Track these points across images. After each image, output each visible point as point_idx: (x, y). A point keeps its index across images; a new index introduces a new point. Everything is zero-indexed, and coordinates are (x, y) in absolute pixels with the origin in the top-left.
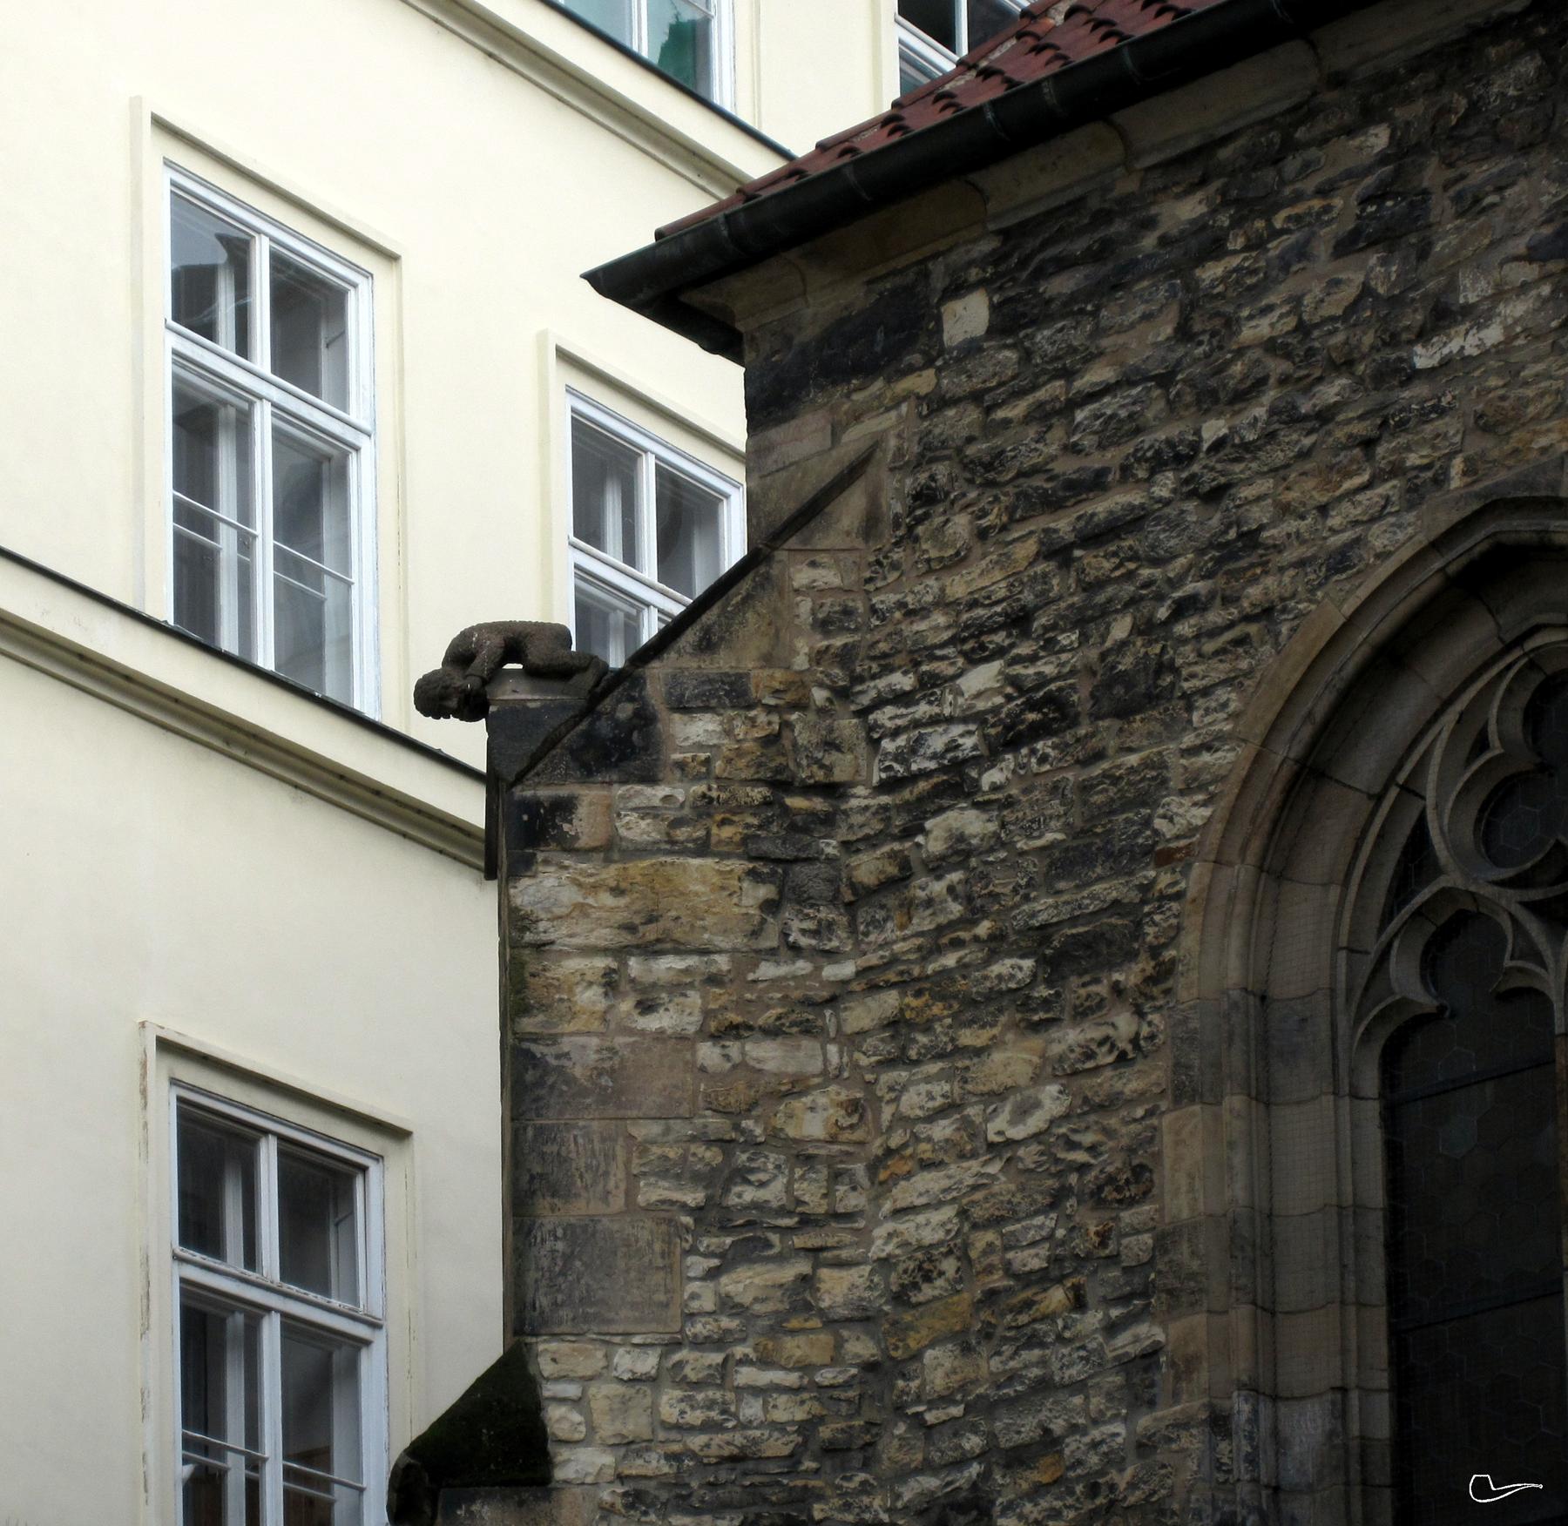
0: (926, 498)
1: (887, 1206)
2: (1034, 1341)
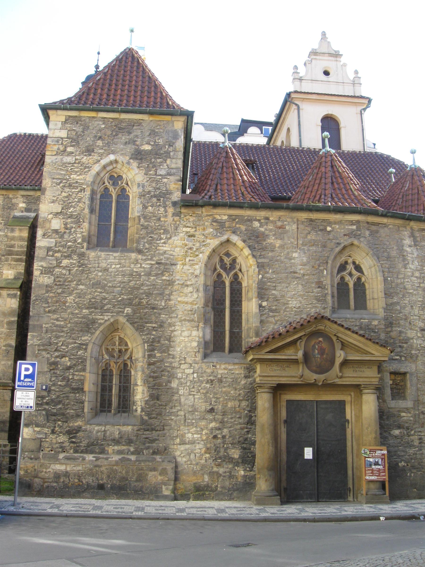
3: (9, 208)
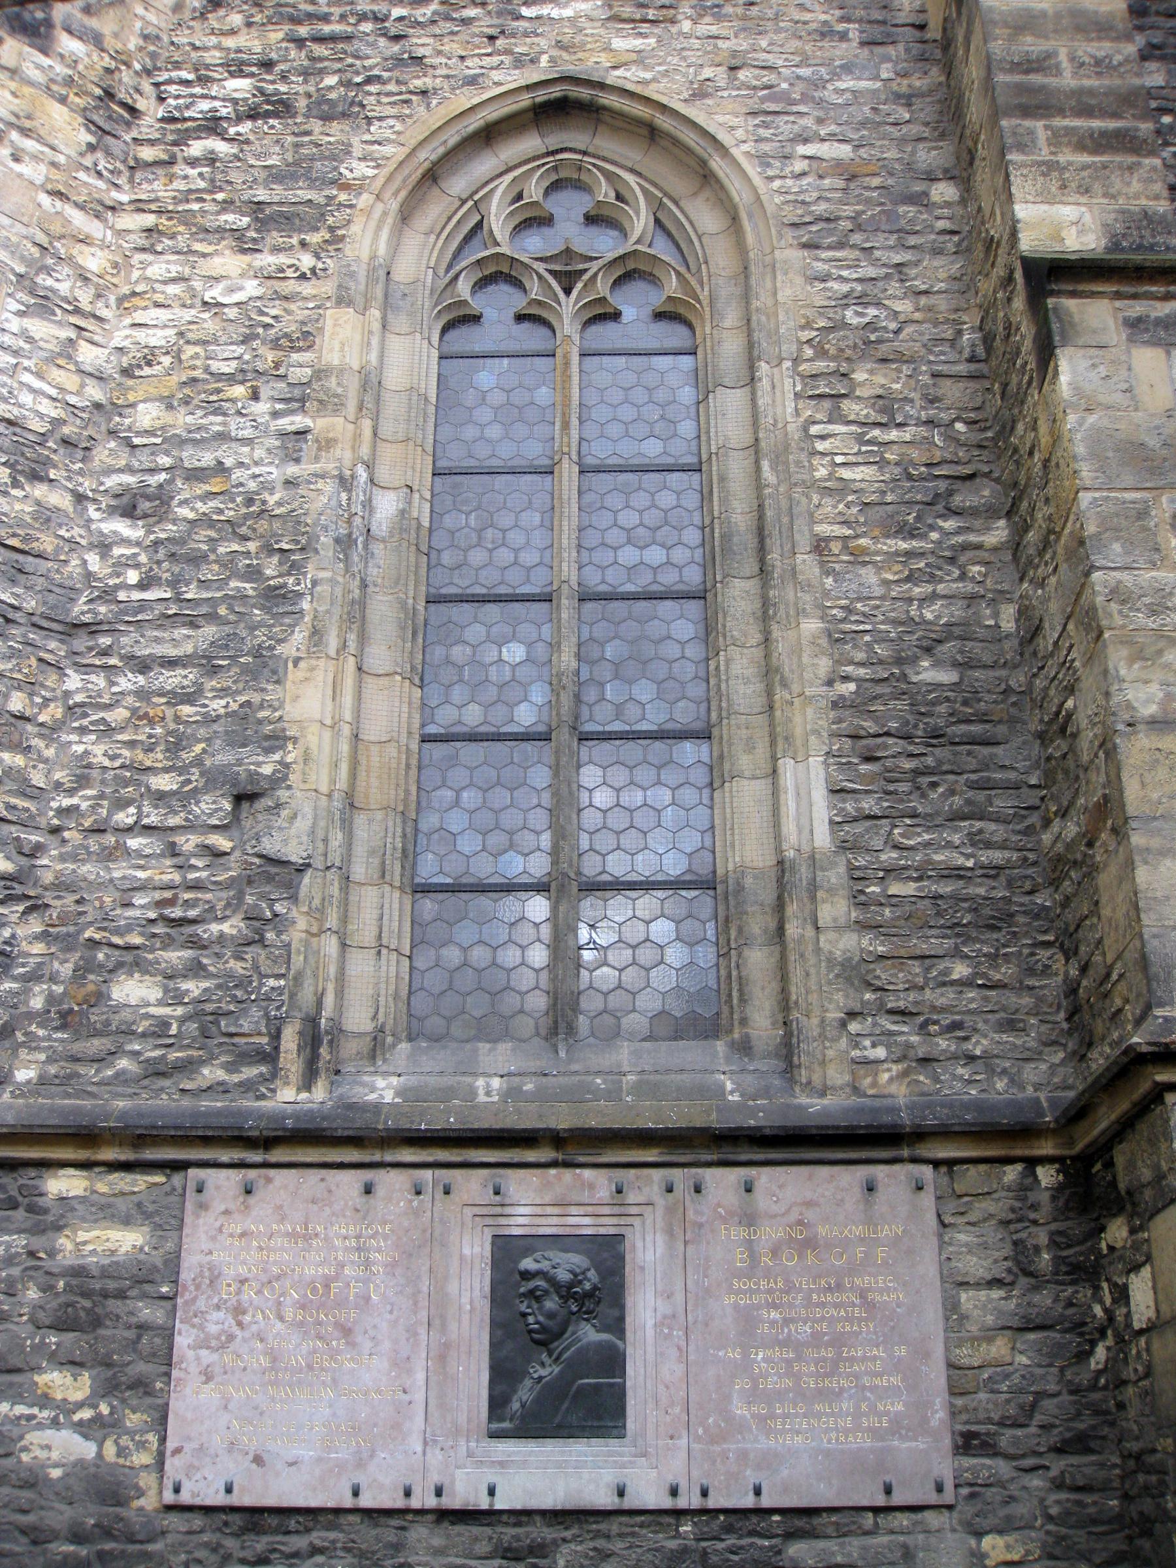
1: (128, 321)
2: (218, 411)
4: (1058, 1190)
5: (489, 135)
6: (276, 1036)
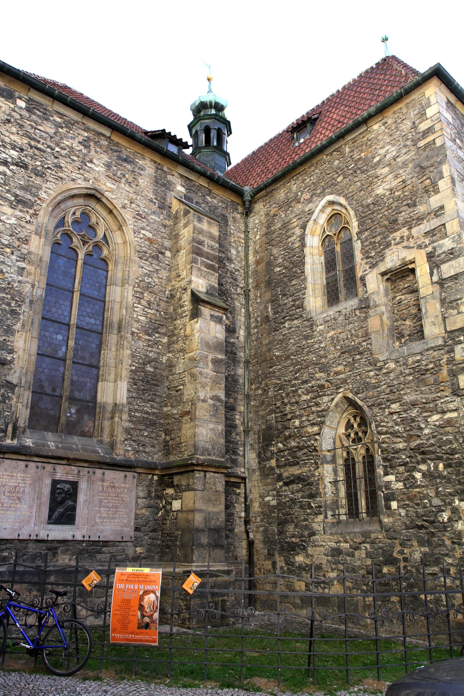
0: (9, 121)
3: (164, 185)
4: (157, 481)
5: (73, 197)
6: (7, 427)
